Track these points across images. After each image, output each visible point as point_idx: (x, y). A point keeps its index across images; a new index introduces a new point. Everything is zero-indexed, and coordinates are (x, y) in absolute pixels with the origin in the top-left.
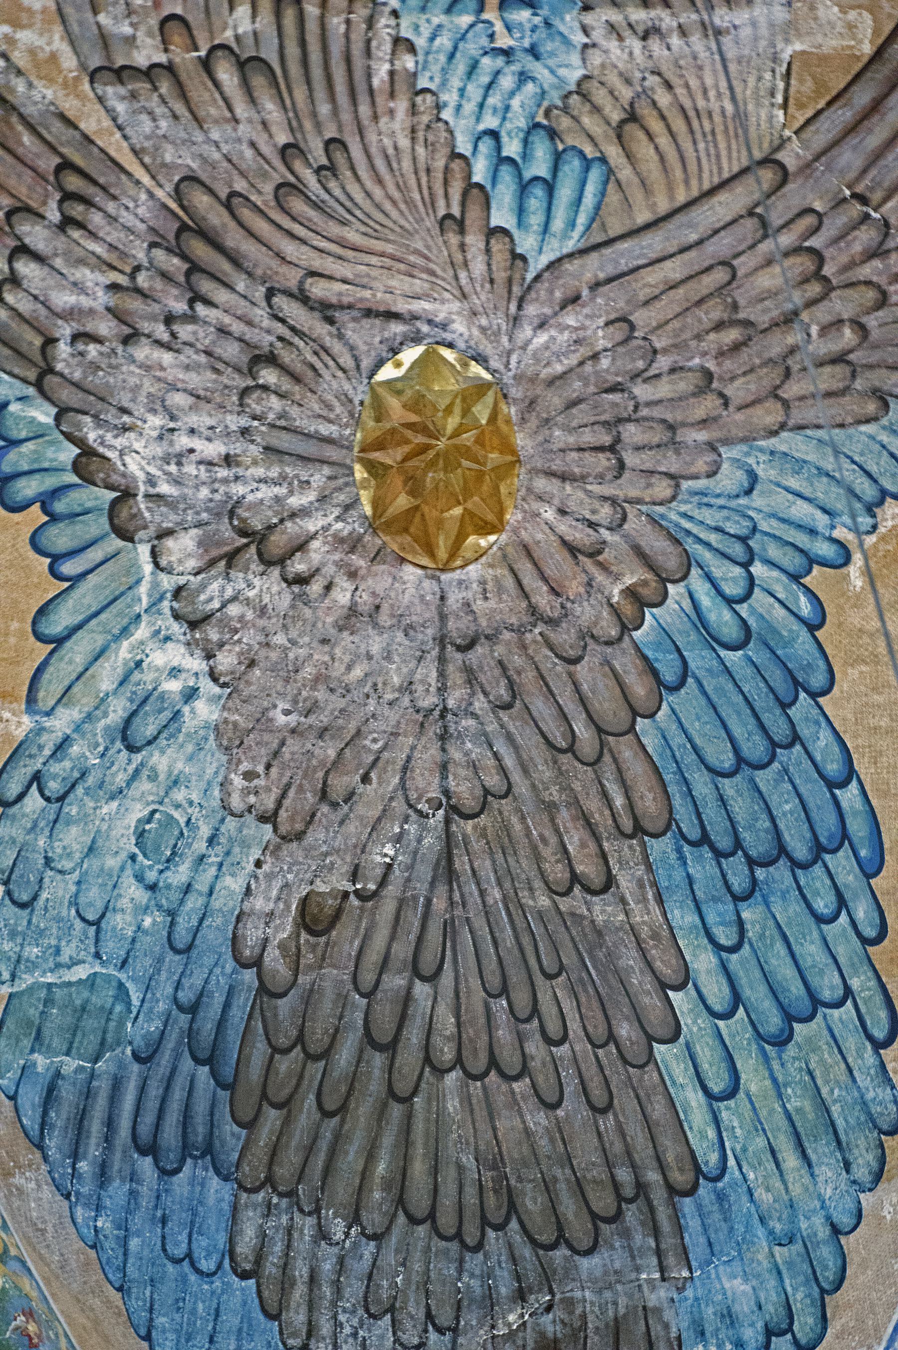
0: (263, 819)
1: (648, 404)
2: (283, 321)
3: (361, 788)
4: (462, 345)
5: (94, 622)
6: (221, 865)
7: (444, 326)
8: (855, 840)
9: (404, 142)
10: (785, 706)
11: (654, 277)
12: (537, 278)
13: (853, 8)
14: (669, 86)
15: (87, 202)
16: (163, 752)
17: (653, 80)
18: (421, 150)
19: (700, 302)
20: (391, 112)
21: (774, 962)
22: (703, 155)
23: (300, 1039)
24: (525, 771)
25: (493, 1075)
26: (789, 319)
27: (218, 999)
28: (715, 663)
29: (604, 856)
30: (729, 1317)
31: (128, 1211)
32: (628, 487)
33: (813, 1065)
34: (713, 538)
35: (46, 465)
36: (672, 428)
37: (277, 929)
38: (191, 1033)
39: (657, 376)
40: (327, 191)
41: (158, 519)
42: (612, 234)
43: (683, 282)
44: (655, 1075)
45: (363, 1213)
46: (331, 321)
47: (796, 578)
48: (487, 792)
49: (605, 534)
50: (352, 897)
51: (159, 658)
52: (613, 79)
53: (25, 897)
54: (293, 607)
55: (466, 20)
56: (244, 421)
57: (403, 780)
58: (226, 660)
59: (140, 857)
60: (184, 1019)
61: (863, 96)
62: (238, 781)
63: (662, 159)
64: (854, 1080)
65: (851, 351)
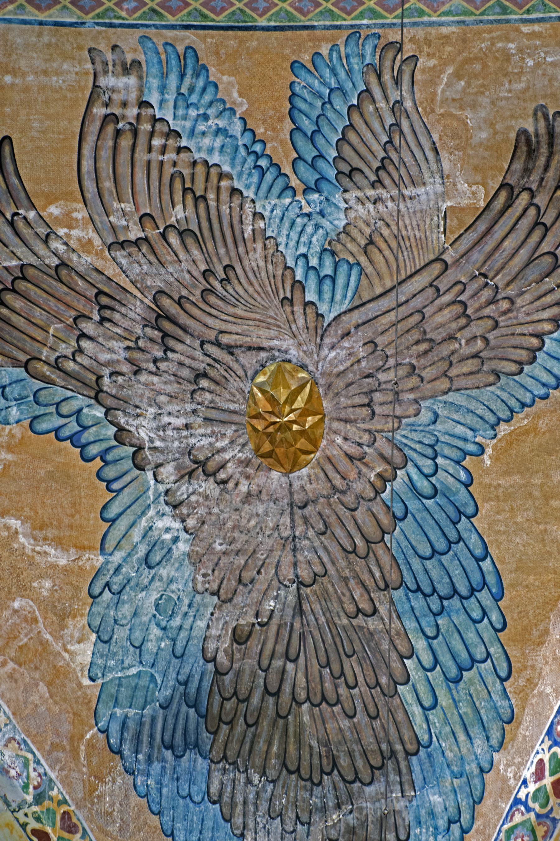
0: (213, 594)
1: (385, 382)
2: (209, 356)
3: (257, 577)
5: (129, 510)
6: (195, 616)
7: (286, 352)
8: (490, 585)
9: (262, 264)
10: (455, 524)
12: (329, 325)
13: (475, 184)
14: (388, 225)
15: (112, 309)
16: (164, 568)
17: (380, 223)
18: (270, 267)
19: (408, 331)
20: (255, 249)
21: (454, 642)
22: (406, 258)
23: (235, 693)
24: (333, 563)
27: (197, 677)
29: (372, 600)
30: (432, 814)
31: (161, 776)
32: (376, 425)
33: (472, 692)
34: (418, 447)
35: (102, 437)
36: (397, 393)
37: (223, 643)
38: (185, 695)
39: (389, 369)
41: (155, 459)
42: (364, 300)
44: (398, 700)
45: (267, 771)
46: (232, 354)
47: (458, 463)
48: (315, 575)
49: (366, 449)
50: (256, 625)
51: (160, 524)
52: (361, 224)
53: (106, 638)
55: (288, 201)
56: (194, 406)
57: (276, 572)
58: (191, 522)
59: (158, 615)
60: (182, 688)
61: (482, 227)
62: (200, 578)
63: (387, 261)
64: (491, 697)
65: (481, 352)
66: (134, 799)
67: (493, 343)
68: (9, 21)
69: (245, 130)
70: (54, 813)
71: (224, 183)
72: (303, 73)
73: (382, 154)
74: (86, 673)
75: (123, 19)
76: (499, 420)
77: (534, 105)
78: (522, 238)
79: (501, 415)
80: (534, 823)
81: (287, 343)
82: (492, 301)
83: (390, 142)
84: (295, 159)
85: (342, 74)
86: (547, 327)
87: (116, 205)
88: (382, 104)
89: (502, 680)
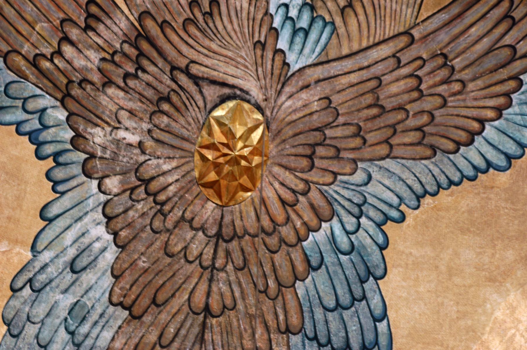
0: (125, 308)
1: (331, 138)
2: (176, 82)
8: (381, 346)
11: (345, 80)
18: (252, 9)
24: (244, 299)
26: (401, 108)
28: (336, 260)
29: (270, 340)
32: (314, 176)
34: (346, 204)
35: (59, 139)
36: (338, 150)
40: (207, 24)
42: (331, 57)
43: (357, 84)
46: (197, 84)
47: (379, 225)
48: (224, 307)
53: (16, 332)
67: (438, 120)
76: (426, 192)
78: (489, 27)
82: (446, 81)
86: (490, 114)
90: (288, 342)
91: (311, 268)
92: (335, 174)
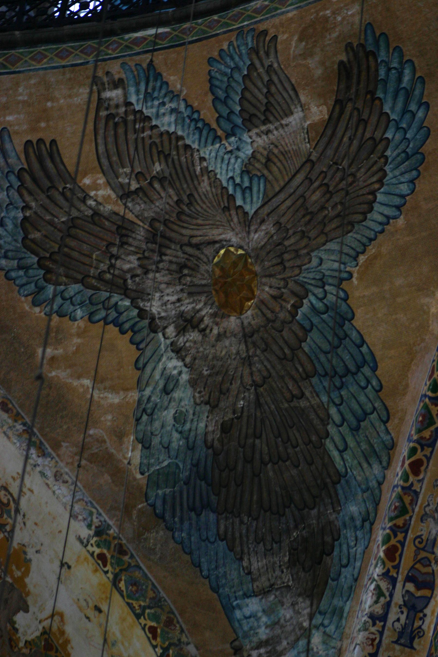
1: (290, 246)
4: (235, 245)
9: (208, 188)
11: (284, 207)
12: (252, 218)
14: (276, 147)
17: (272, 146)
18: (214, 190)
19: (297, 210)
20: (203, 181)
25: (280, 462)
26: (323, 208)
27: (203, 460)
30: (352, 519)
32: (288, 273)
34: (313, 282)
37: (217, 435)
39: (290, 237)
40: (191, 210)
46: (199, 249)
49: (283, 290)
52: (261, 150)
53: (147, 445)
54: (203, 339)
55: (218, 145)
56: (181, 287)
57: (241, 381)
58: (188, 360)
60: (195, 469)
62: (197, 395)
64: (379, 435)
66: (172, 544)
68: (45, 69)
69: (187, 106)
70: (110, 543)
71: (180, 143)
72: (215, 64)
73: (265, 101)
74: (138, 470)
75: (110, 54)
77: (345, 44)
79: (359, 250)
80: (402, 494)
81: (228, 235)
83: (269, 92)
84: (218, 117)
85: (237, 58)
86: (377, 186)
87: (121, 171)
88: (261, 70)
89: (385, 423)
90: (311, 383)
91: (306, 331)
92: (300, 267)
